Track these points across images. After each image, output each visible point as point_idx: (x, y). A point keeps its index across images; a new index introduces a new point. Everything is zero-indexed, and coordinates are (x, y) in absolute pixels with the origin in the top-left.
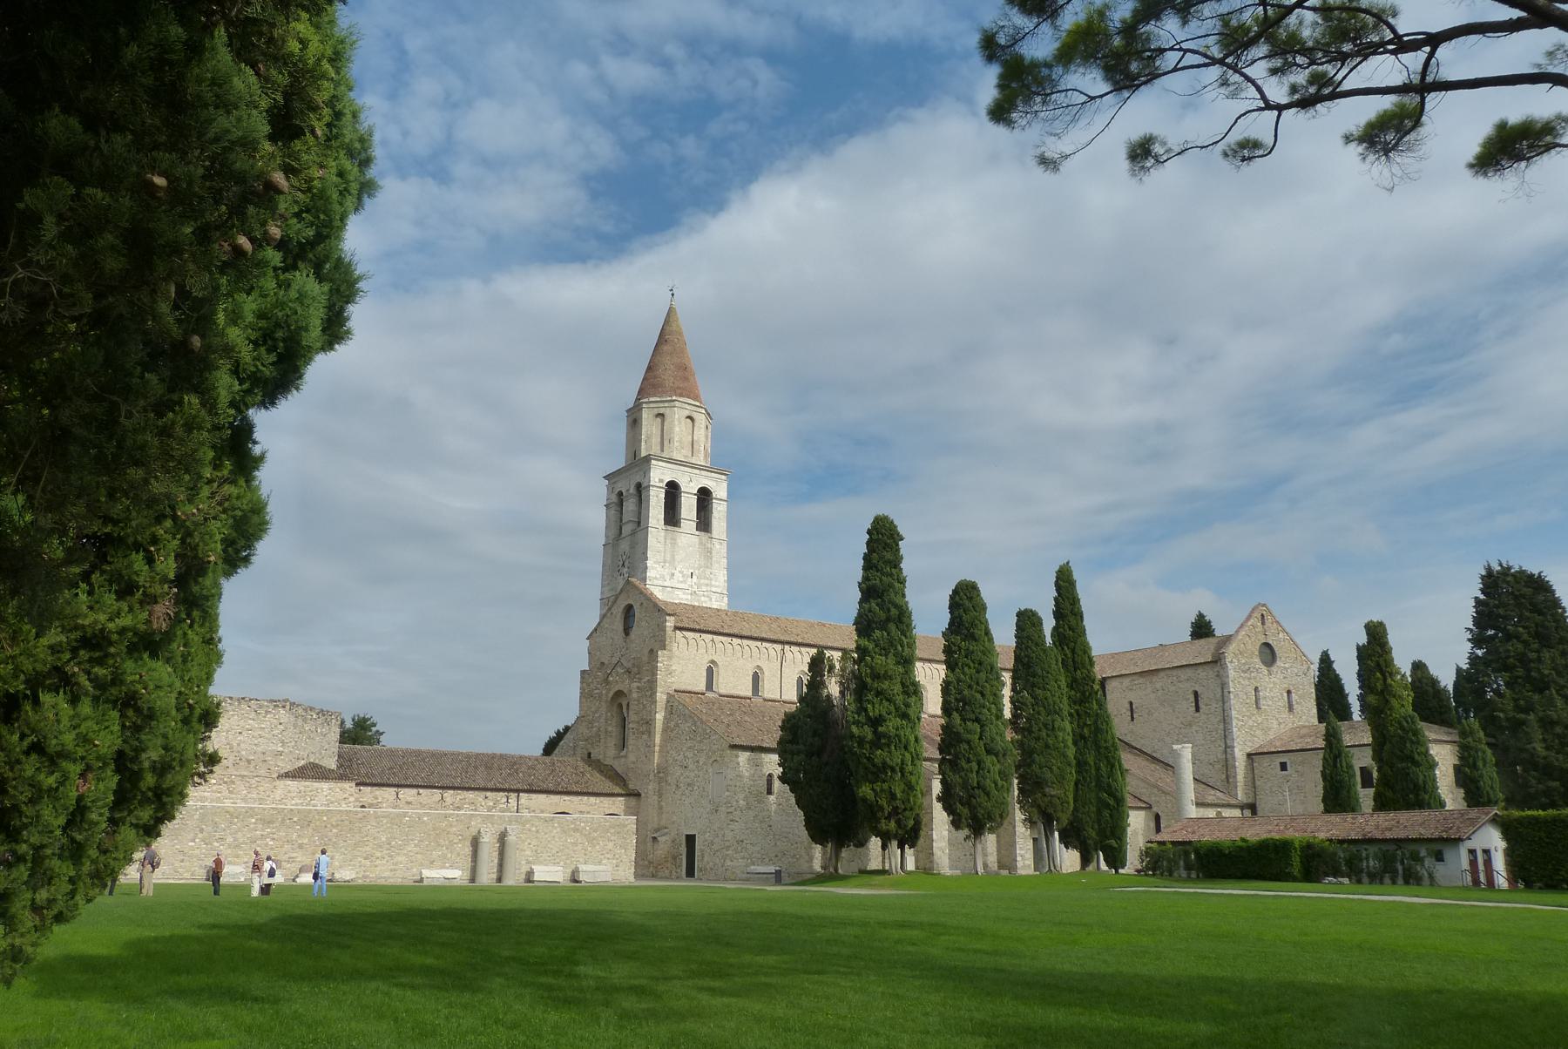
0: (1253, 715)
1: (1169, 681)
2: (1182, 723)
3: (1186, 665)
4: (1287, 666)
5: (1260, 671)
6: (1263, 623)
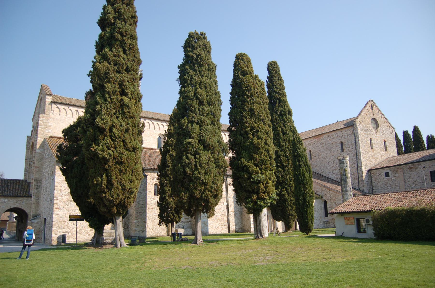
0: (370, 151)
1: (328, 139)
2: (335, 158)
3: (337, 130)
4: (383, 129)
5: (372, 131)
6: (372, 109)
